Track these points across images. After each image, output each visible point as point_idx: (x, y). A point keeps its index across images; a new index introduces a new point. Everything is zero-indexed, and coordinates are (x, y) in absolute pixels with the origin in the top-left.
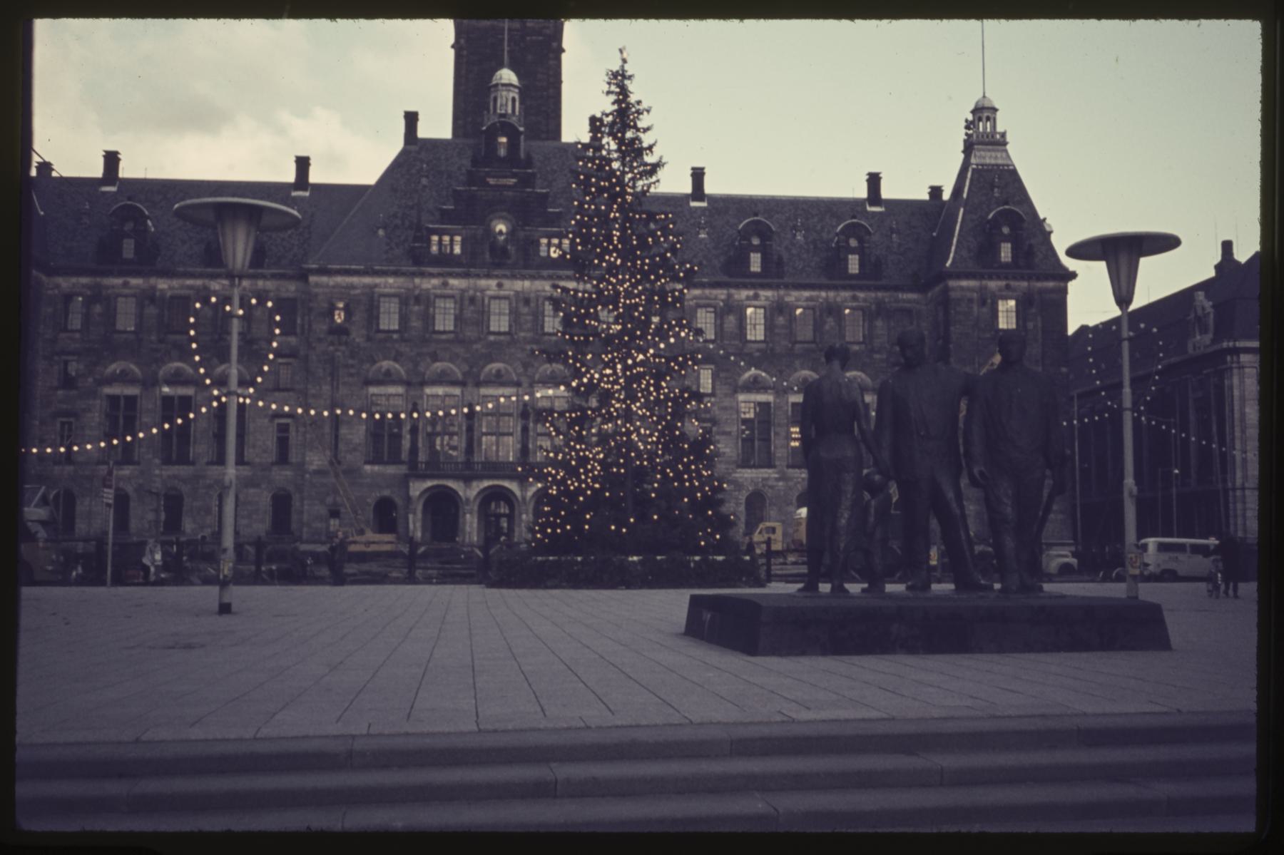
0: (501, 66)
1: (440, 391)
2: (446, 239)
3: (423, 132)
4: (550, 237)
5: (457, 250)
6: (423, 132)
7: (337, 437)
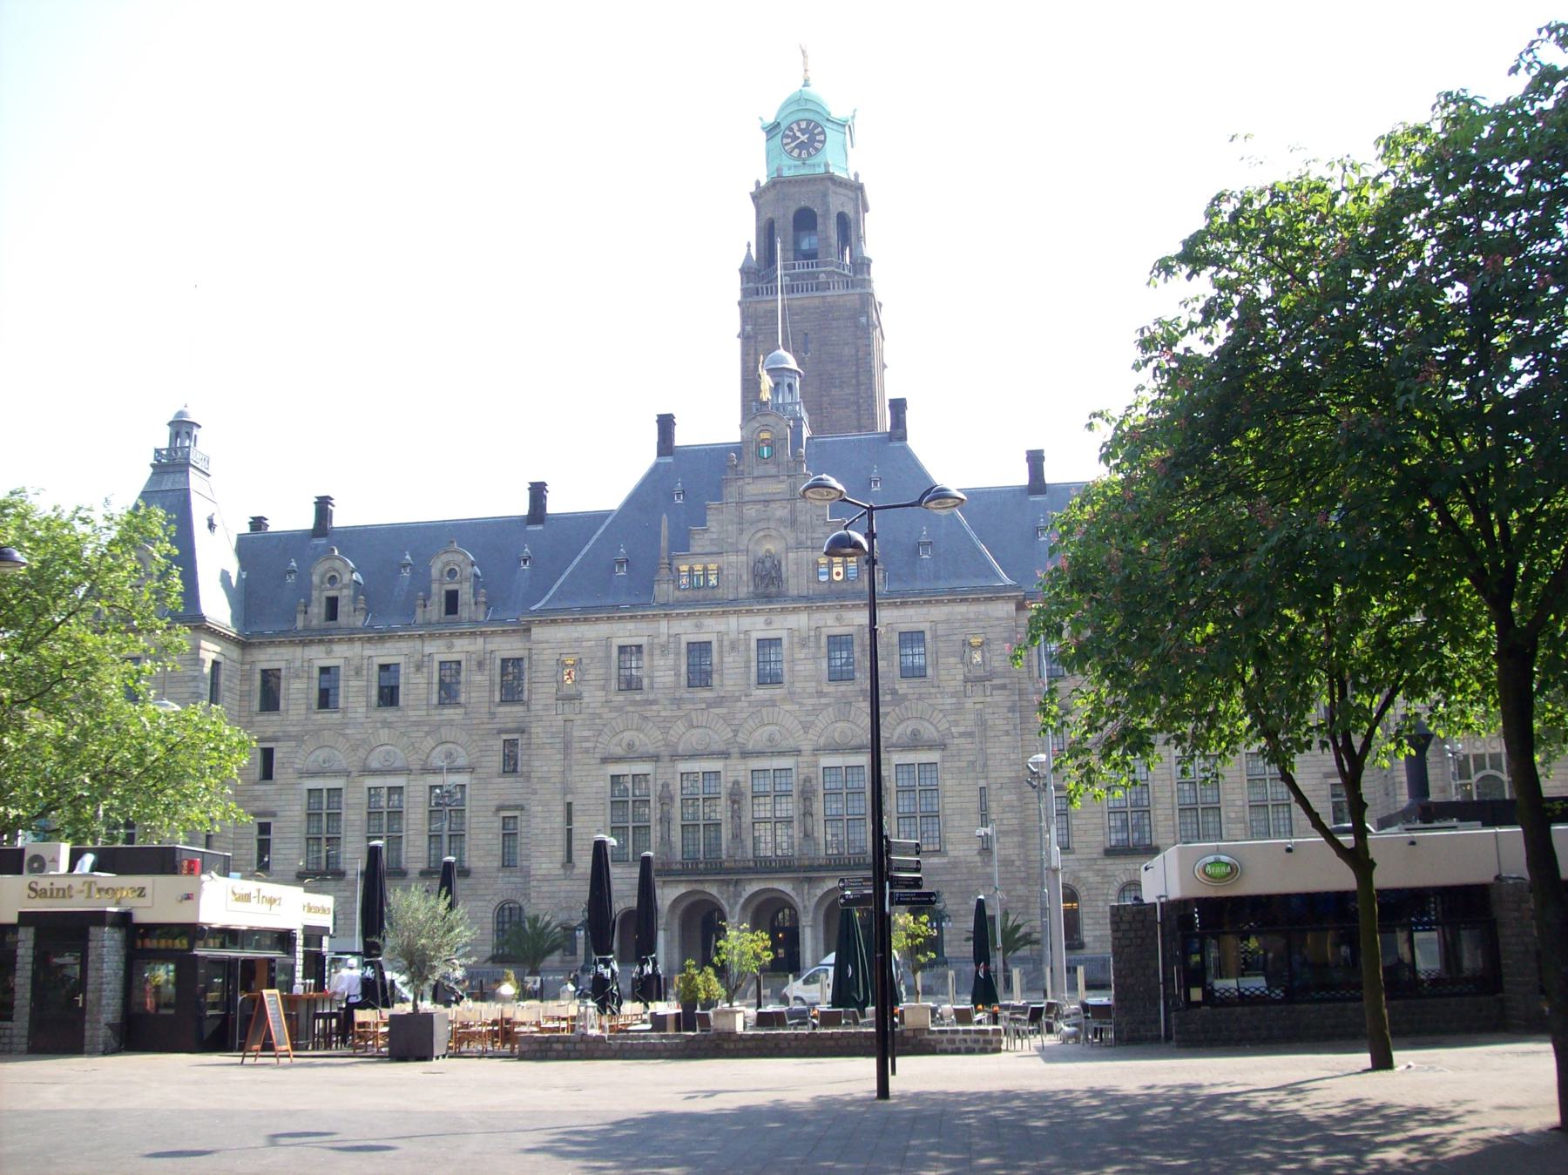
3: (683, 437)
6: (682, 438)
7: (570, 831)
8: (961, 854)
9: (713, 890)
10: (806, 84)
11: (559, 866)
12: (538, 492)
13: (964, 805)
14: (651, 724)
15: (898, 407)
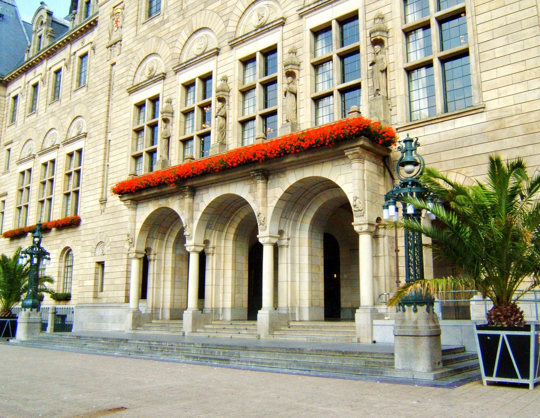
8: (511, 101)
11: (98, 202)
13: (510, 19)
14: (163, 42)
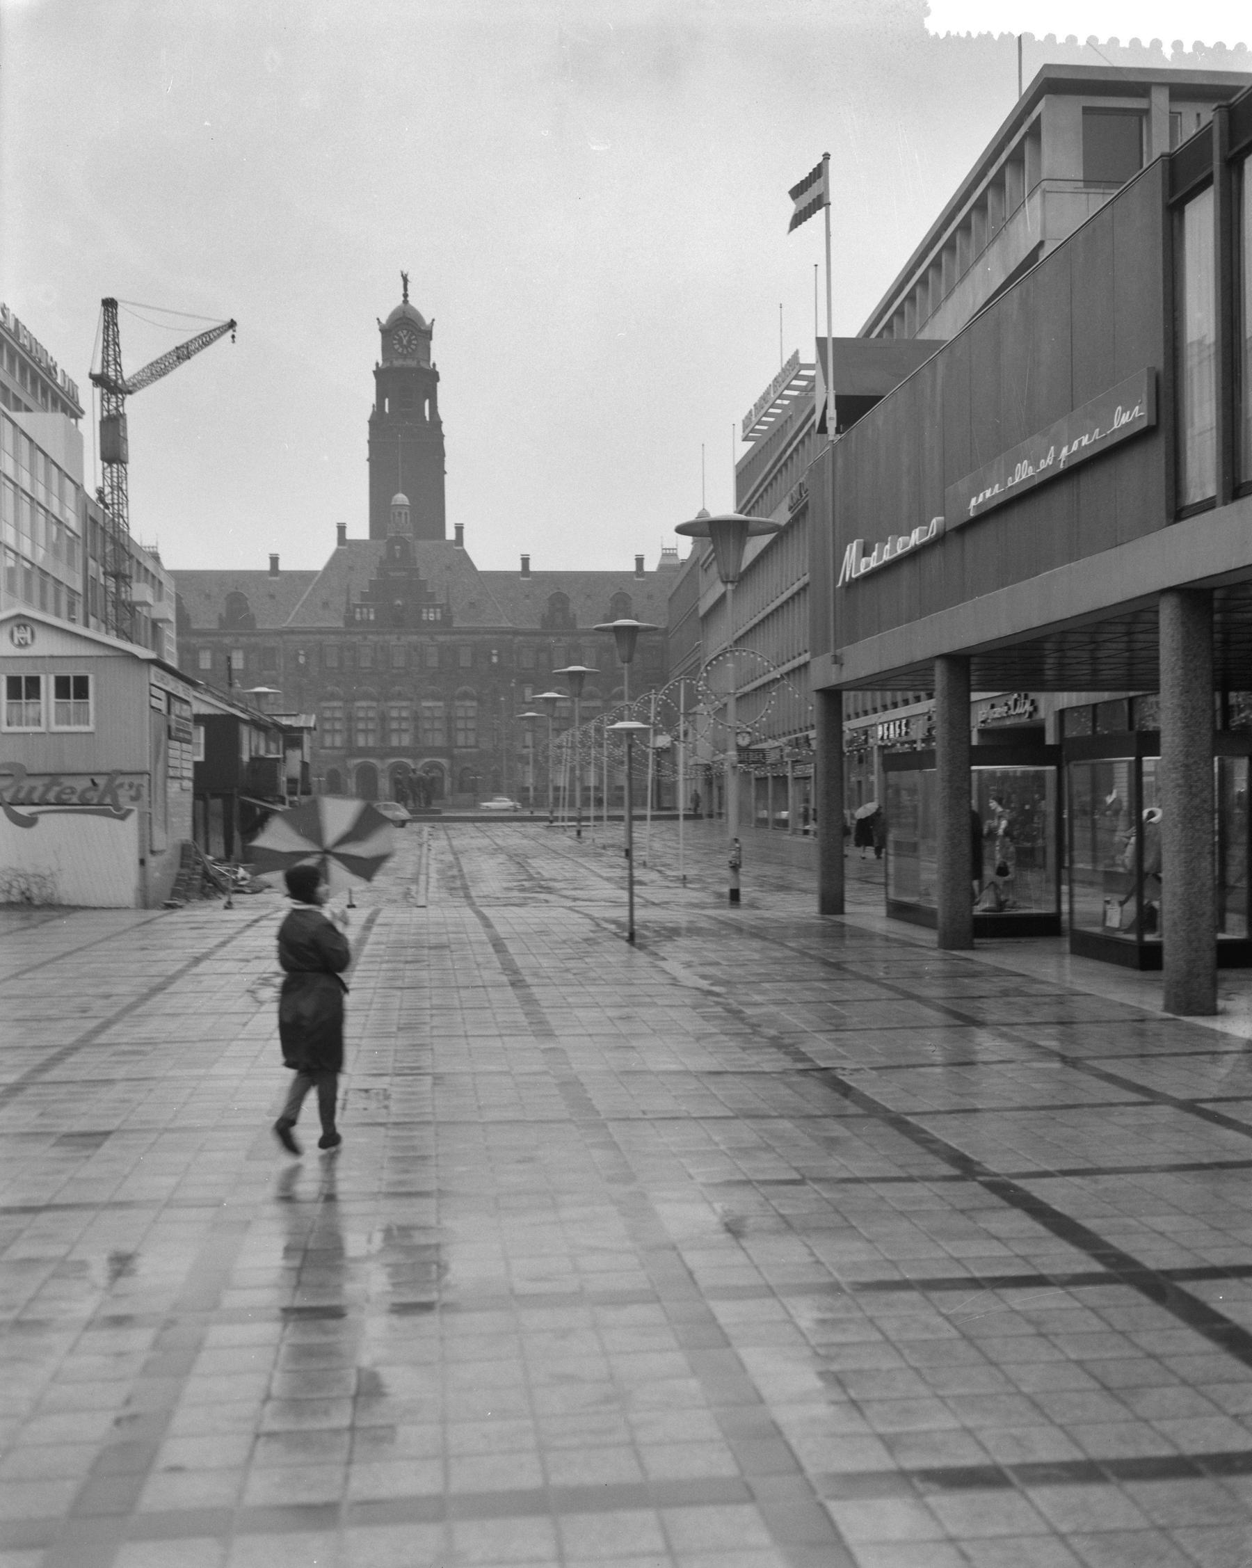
0: (397, 492)
1: (364, 704)
2: (365, 610)
3: (350, 535)
4: (428, 607)
5: (372, 617)
6: (350, 535)
9: (372, 760)
10: (405, 301)
12: (274, 560)
15: (459, 529)
